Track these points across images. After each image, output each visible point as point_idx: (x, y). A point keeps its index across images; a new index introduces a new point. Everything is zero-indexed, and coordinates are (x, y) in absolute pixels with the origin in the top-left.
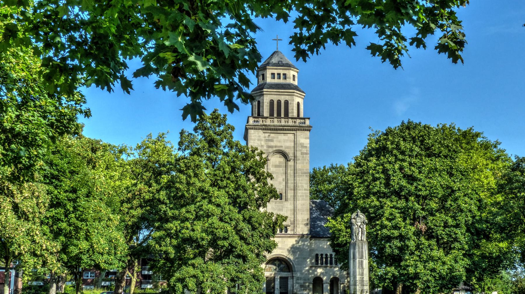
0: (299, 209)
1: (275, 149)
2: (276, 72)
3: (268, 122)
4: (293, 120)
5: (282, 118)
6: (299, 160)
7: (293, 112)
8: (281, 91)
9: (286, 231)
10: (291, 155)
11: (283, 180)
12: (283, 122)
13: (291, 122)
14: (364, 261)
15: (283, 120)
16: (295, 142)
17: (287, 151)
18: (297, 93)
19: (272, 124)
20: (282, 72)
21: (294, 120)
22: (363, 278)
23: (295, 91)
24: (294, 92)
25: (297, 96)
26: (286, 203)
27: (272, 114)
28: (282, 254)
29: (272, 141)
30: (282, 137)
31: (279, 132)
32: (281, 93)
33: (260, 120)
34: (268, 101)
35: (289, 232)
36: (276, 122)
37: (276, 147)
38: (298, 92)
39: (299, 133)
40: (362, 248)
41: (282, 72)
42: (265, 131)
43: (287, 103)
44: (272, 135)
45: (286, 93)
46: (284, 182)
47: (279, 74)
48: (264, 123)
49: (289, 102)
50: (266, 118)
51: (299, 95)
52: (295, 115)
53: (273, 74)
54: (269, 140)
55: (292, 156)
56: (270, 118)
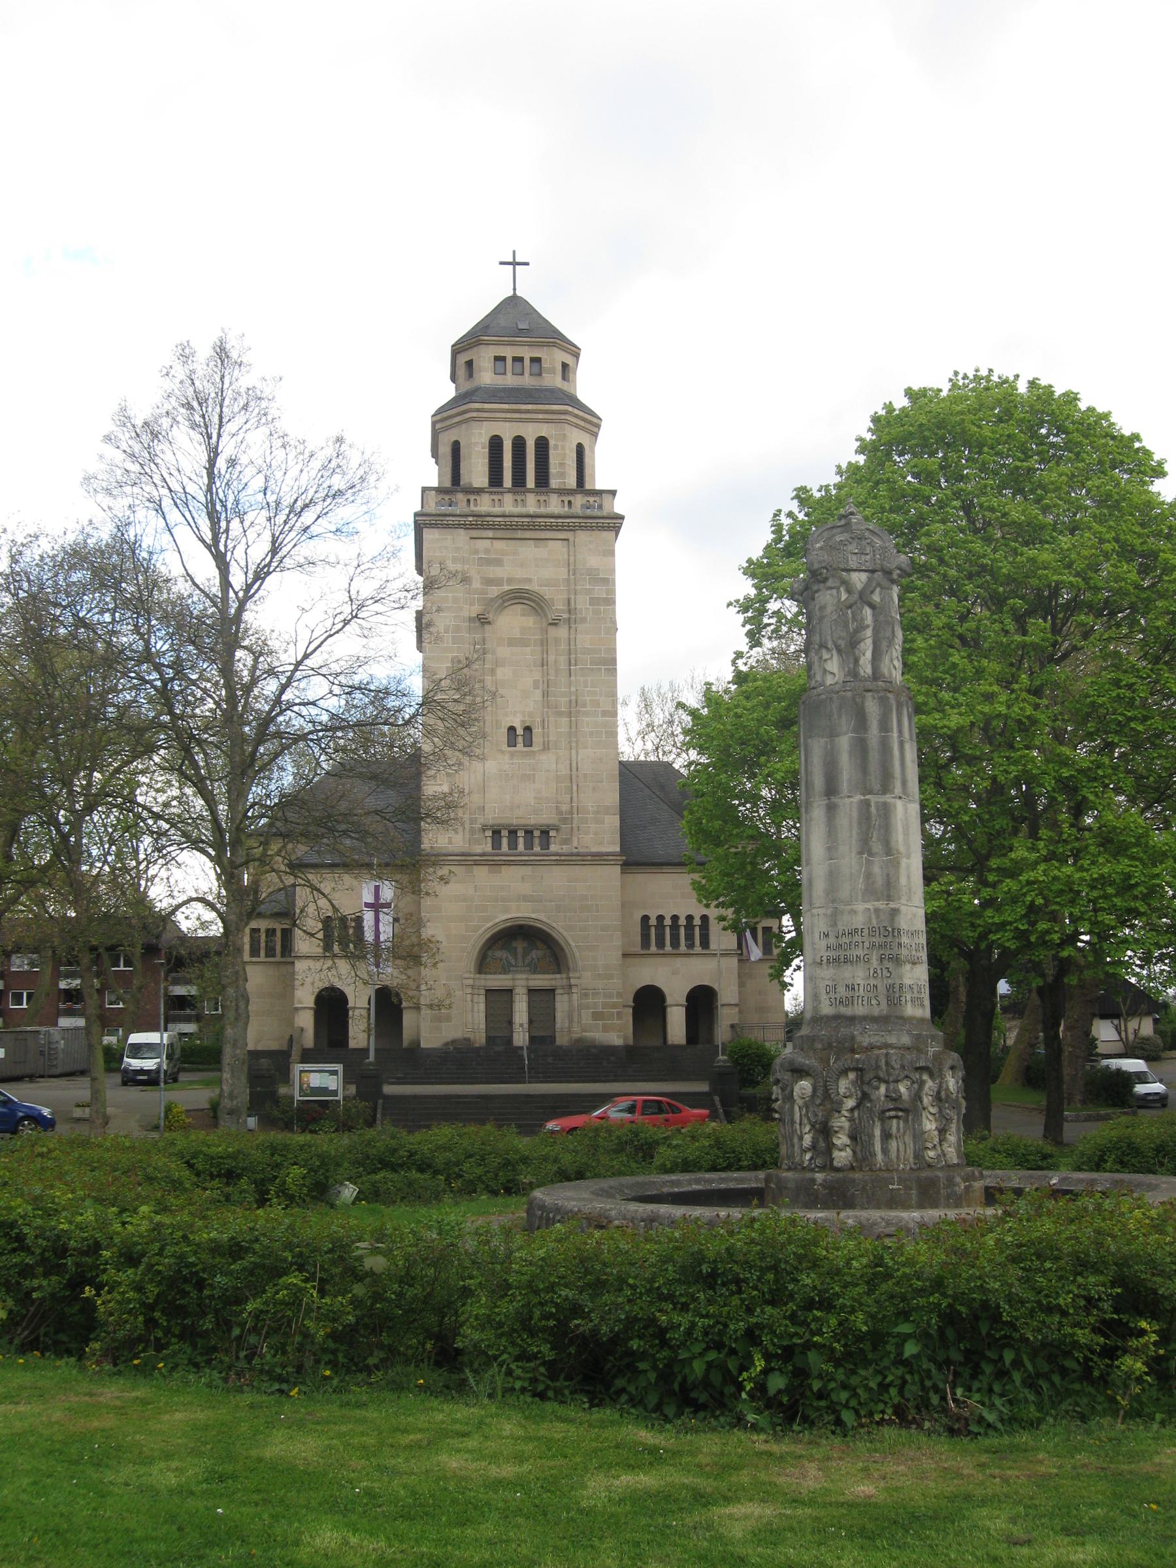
0: (585, 775)
1: (506, 588)
2: (509, 352)
3: (484, 504)
4: (563, 498)
5: (530, 491)
6: (584, 620)
7: (562, 475)
8: (524, 407)
9: (546, 845)
10: (557, 598)
11: (536, 685)
12: (531, 504)
13: (555, 505)
14: (899, 804)
15: (531, 499)
16: (572, 569)
17: (547, 592)
18: (576, 416)
19: (497, 510)
20: (527, 353)
21: (566, 499)
22: (895, 912)
23: (570, 409)
24: (566, 413)
25: (577, 426)
26: (543, 757)
27: (495, 477)
28: (533, 916)
29: (499, 562)
30: (529, 551)
31: (520, 534)
32: (523, 416)
33: (461, 497)
34: (485, 440)
35: (553, 848)
36: (509, 504)
37: (510, 581)
38: (576, 412)
39: (582, 537)
40: (885, 726)
41: (527, 353)
42: (475, 533)
43: (542, 445)
44: (499, 545)
45: (541, 416)
46: (538, 693)
47: (518, 360)
48: (472, 508)
49: (552, 443)
50: (479, 491)
51: (582, 423)
52: (572, 482)
53: (500, 359)
54: (489, 562)
55: (563, 611)
56: (491, 493)
